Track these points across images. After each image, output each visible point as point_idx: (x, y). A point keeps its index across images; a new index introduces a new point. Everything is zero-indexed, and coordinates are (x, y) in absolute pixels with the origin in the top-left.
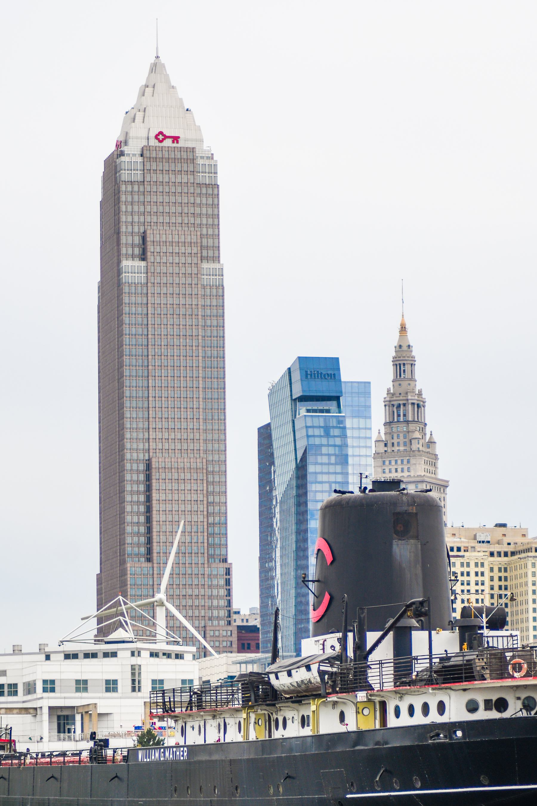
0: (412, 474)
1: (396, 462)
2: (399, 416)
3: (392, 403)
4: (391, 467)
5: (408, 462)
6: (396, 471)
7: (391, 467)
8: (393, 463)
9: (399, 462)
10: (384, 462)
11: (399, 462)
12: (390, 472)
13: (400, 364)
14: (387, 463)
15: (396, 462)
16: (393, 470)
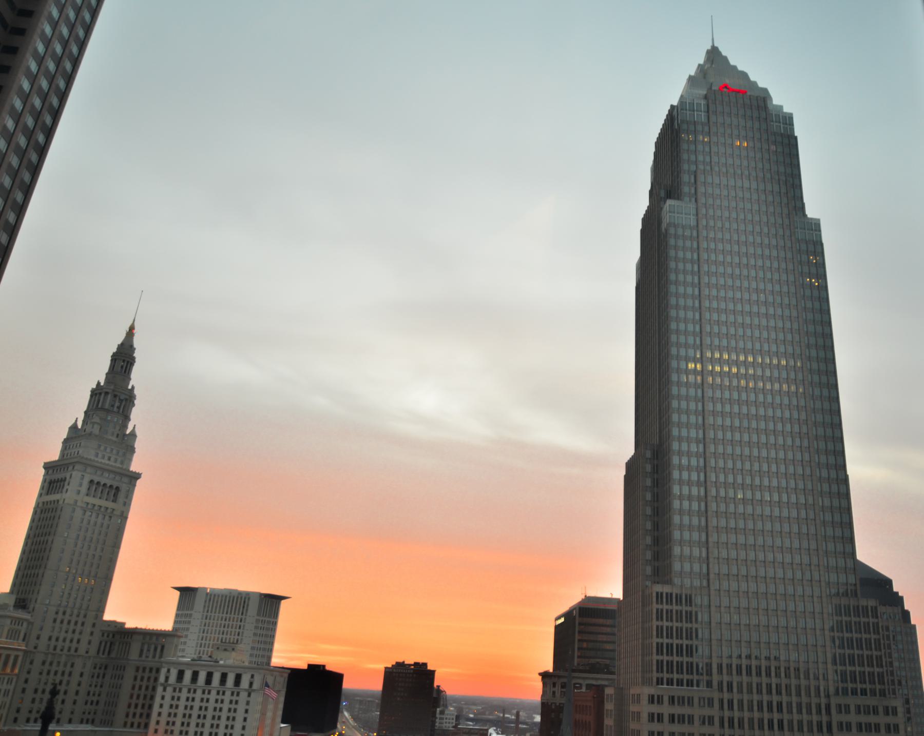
0: (125, 467)
1: (112, 450)
2: (119, 408)
3: (116, 393)
4: (105, 453)
5: (124, 454)
6: (109, 459)
7: (105, 453)
8: (108, 450)
9: (114, 452)
10: (100, 446)
11: (114, 452)
12: (103, 457)
13: (128, 362)
14: (102, 448)
15: (112, 450)
16: (106, 458)
